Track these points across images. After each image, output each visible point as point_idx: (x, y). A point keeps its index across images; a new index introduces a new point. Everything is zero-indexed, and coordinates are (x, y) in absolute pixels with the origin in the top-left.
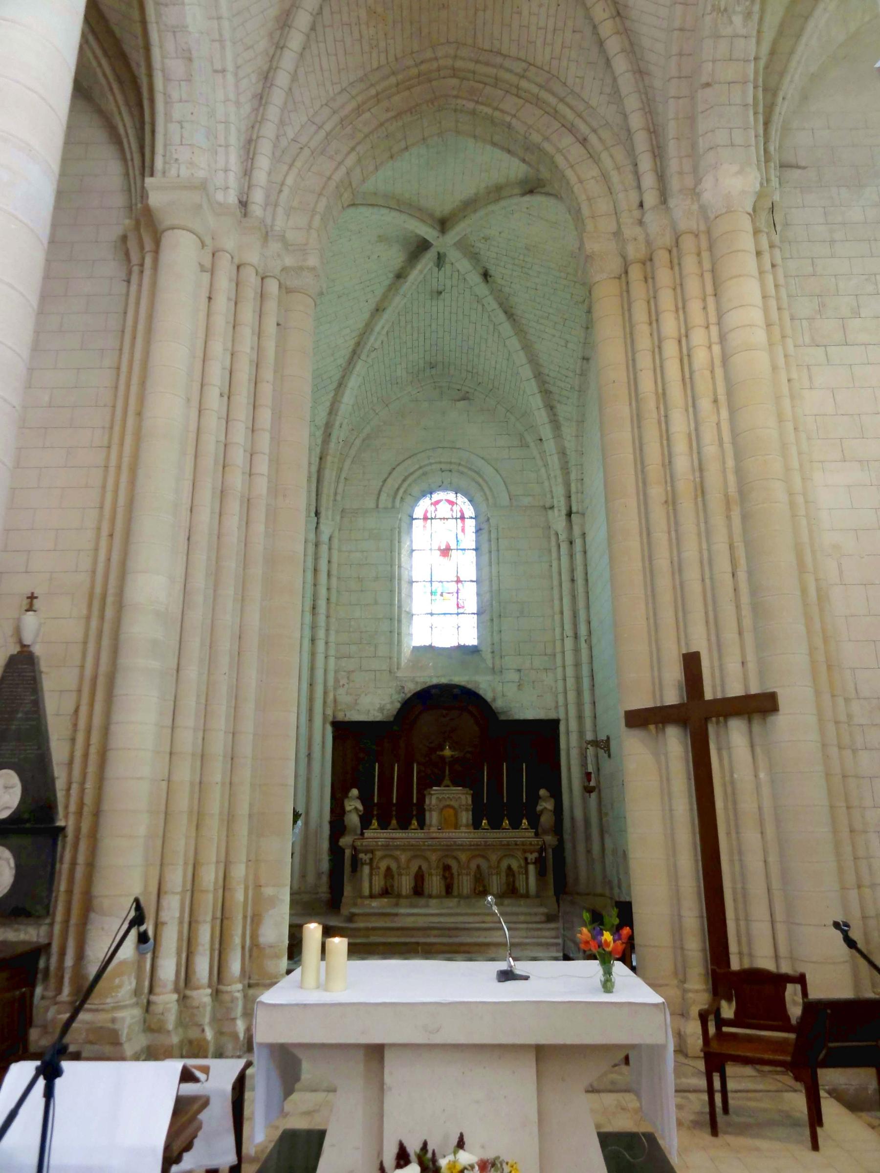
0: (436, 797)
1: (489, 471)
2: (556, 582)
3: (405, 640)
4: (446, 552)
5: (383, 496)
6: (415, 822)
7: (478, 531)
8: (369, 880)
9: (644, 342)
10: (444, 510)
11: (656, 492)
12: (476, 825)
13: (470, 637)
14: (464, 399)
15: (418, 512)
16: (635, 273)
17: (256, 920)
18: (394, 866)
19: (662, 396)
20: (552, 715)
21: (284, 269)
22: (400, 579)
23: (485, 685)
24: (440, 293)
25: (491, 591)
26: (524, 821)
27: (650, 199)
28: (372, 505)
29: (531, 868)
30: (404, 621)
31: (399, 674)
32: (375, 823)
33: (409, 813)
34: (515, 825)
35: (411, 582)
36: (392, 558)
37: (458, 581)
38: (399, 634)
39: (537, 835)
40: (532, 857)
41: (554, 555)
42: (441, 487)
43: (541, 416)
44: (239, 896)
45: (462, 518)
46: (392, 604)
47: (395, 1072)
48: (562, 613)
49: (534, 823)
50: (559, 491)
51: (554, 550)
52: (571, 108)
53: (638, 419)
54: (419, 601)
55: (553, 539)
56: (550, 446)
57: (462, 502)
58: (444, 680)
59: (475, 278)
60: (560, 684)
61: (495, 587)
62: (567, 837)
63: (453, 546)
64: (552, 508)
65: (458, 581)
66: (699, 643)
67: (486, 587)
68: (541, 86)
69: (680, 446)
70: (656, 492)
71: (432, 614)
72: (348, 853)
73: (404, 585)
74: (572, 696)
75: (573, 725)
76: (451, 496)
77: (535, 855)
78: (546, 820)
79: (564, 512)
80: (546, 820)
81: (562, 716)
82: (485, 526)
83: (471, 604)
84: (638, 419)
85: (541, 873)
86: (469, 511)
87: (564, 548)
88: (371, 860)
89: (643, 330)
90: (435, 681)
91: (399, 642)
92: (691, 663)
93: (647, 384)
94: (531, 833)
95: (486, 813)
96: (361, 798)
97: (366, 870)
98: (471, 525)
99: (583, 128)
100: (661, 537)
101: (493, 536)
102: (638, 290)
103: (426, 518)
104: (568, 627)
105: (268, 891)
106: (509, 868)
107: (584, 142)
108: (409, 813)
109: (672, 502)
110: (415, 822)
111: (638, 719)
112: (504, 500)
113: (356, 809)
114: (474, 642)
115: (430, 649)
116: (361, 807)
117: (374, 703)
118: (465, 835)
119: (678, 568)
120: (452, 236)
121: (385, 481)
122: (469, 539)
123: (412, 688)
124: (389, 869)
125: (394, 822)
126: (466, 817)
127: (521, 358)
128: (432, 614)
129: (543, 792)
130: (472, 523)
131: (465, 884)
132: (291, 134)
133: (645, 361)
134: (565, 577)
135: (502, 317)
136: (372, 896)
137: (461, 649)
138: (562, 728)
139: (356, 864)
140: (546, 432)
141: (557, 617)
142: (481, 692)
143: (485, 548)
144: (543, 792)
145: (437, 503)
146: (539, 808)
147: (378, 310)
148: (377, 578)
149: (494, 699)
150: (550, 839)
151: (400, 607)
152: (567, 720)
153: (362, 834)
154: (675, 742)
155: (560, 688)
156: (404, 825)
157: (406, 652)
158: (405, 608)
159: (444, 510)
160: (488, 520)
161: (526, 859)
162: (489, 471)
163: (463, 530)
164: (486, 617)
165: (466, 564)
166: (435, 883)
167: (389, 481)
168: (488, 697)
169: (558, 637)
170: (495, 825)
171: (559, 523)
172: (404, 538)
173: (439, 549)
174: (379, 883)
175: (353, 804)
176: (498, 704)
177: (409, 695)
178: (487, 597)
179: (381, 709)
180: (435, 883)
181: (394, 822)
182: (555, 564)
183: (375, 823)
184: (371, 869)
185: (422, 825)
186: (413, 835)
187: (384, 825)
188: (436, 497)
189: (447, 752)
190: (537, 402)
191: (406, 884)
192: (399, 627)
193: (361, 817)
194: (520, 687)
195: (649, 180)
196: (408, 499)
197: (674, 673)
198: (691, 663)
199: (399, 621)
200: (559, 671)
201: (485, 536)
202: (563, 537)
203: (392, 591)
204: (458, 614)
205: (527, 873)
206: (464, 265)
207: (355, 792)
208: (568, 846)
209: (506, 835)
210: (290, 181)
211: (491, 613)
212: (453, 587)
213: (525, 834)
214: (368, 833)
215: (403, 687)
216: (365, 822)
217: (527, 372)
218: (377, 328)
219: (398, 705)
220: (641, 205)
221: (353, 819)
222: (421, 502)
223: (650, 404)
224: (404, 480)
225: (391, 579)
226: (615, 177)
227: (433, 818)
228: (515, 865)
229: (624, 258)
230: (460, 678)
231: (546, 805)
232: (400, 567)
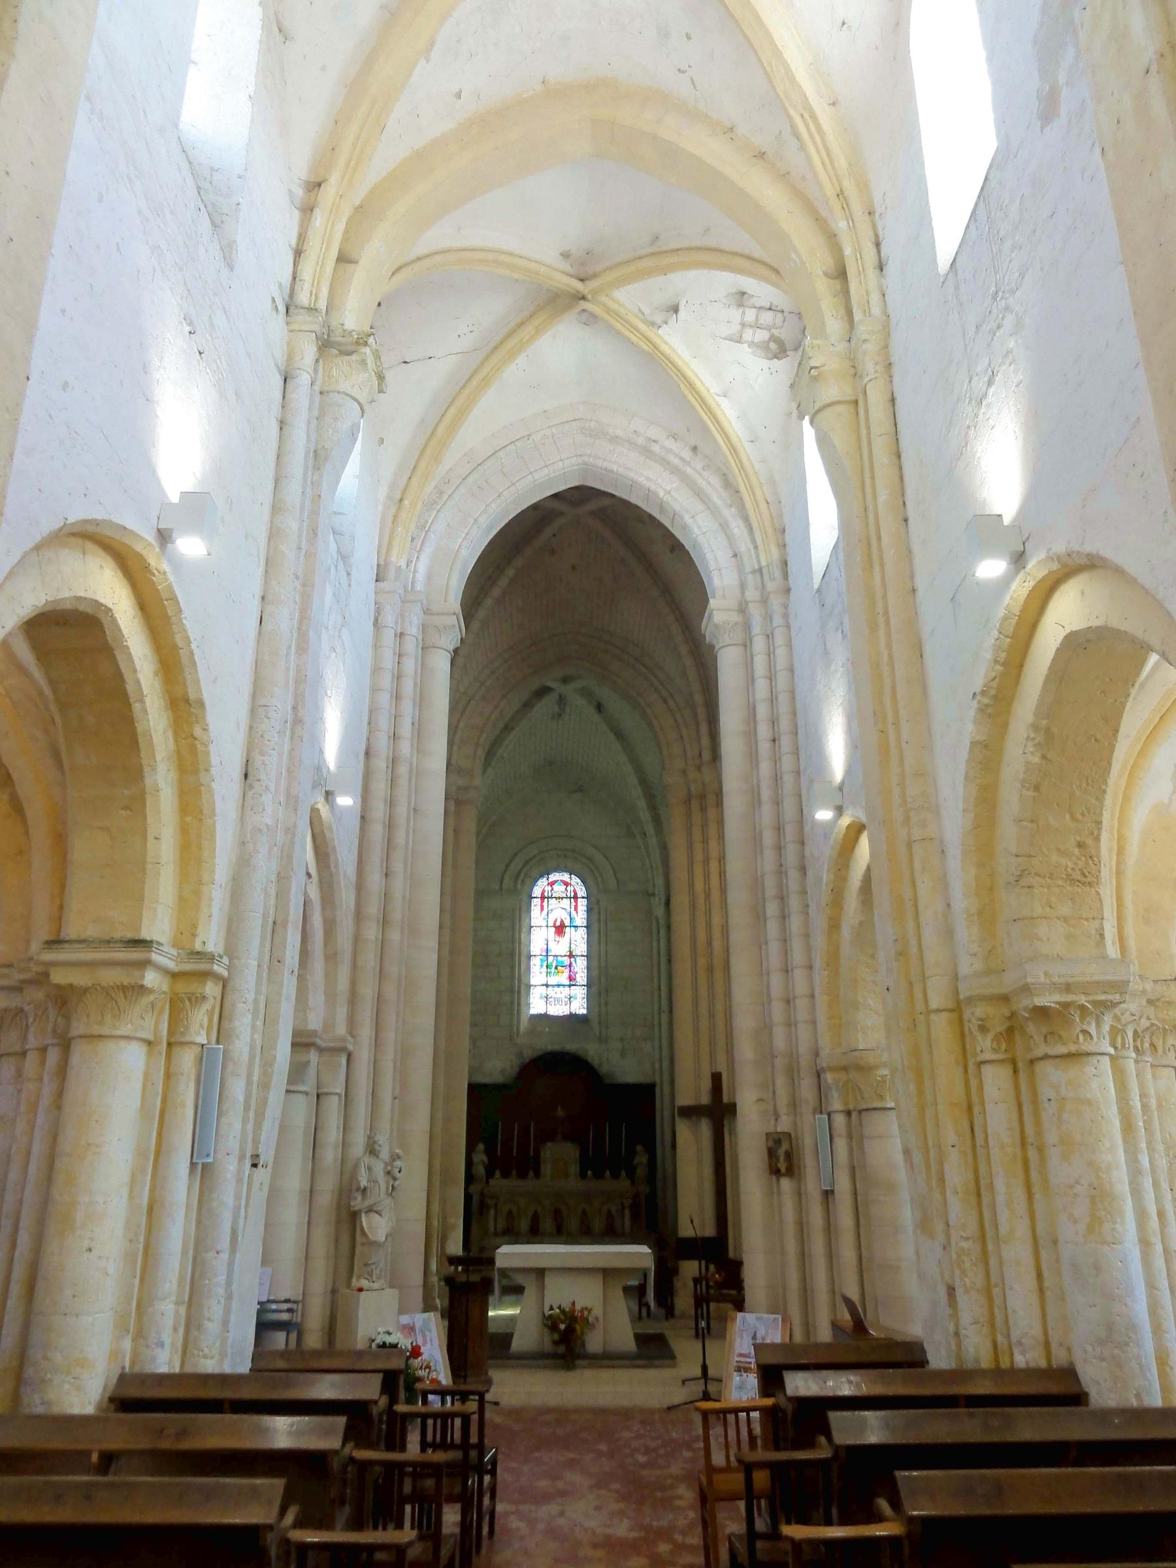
0: (550, 1151)
1: (598, 857)
2: (655, 961)
3: (523, 1009)
4: (560, 929)
5: (506, 881)
6: (531, 1174)
7: (589, 910)
8: (492, 1221)
9: (699, 856)
10: (559, 889)
11: (702, 962)
12: (583, 1175)
13: (579, 1007)
14: (580, 790)
15: (537, 891)
16: (695, 804)
17: (444, 1239)
18: (514, 1210)
19: (708, 895)
20: (648, 1080)
21: (459, 788)
22: (520, 955)
23: (592, 1051)
24: (560, 715)
25: (599, 967)
26: (623, 1173)
27: (707, 756)
28: (497, 888)
29: (627, 1212)
30: (523, 991)
31: (519, 1041)
32: (498, 1174)
33: (527, 1165)
34: (615, 1176)
35: (529, 957)
36: (513, 936)
37: (571, 956)
38: (519, 1005)
39: (633, 1183)
40: (628, 1202)
41: (655, 937)
42: (558, 869)
43: (645, 816)
44: (435, 1223)
45: (576, 898)
46: (513, 978)
47: (549, 1280)
48: (659, 989)
49: (631, 1176)
50: (660, 881)
51: (655, 931)
52: (656, 677)
53: (693, 906)
54: (537, 975)
55: (654, 923)
56: (653, 841)
57: (575, 880)
58: (557, 1047)
59: (590, 710)
60: (657, 1052)
61: (603, 965)
62: (659, 1185)
63: (567, 923)
64: (653, 894)
65: (571, 956)
66: (722, 1068)
67: (595, 963)
68: (636, 659)
69: (717, 935)
70: (702, 962)
71: (547, 986)
72: (476, 1199)
73: (523, 959)
74: (666, 1064)
75: (667, 1090)
76: (566, 877)
77: (631, 1201)
78: (641, 1172)
79: (663, 901)
80: (641, 1172)
81: (658, 1080)
82: (596, 907)
83: (582, 977)
84: (693, 906)
85: (635, 1217)
86: (582, 891)
87: (663, 932)
88: (496, 1205)
89: (698, 846)
90: (550, 1048)
91: (519, 1011)
92: (716, 1078)
93: (699, 886)
94: (628, 1183)
95: (592, 1165)
96: (487, 1152)
97: (492, 1212)
98: (582, 904)
99: (664, 692)
100: (703, 992)
101: (603, 917)
102: (697, 818)
103: (543, 898)
104: (664, 1002)
105: (452, 1220)
106: (609, 1212)
107: (665, 702)
108: (527, 1165)
109: (710, 970)
110: (531, 1174)
111: (689, 1112)
112: (612, 884)
113: (483, 1162)
114: (584, 1011)
115: (545, 1017)
116: (484, 1158)
117: (499, 1067)
118: (574, 1183)
119: (712, 1015)
120: (572, 686)
121: (508, 865)
122: (581, 918)
123: (528, 1054)
124: (510, 1213)
125: (514, 1173)
126: (574, 1169)
127: (628, 768)
128: (547, 986)
129: (639, 1148)
130: (585, 902)
131: (573, 1224)
132: (462, 689)
133: (699, 870)
134: (663, 959)
135: (612, 737)
136: (496, 1234)
137: (572, 1017)
138: (658, 1090)
139: (483, 1207)
140: (650, 829)
141: (656, 994)
142: (589, 1059)
143: (595, 926)
144: (639, 1148)
145: (552, 884)
146: (635, 1162)
147: (508, 728)
148: (500, 955)
149: (600, 1065)
150: (644, 1189)
151: (520, 981)
152: (662, 1082)
153: (488, 1182)
154: (705, 1128)
155: (657, 1057)
156: (522, 1175)
157: (524, 1023)
158: (524, 980)
159: (559, 889)
160: (598, 902)
161: (622, 1204)
162: (598, 857)
163: (576, 909)
164: (595, 989)
165: (578, 940)
166: (547, 1224)
167: (513, 865)
168: (595, 1062)
169: (656, 1011)
170: (599, 1176)
171: (659, 911)
172: (523, 915)
173: (554, 926)
174: (501, 1224)
175: (480, 1157)
176: (604, 1069)
177: (527, 1061)
178: (595, 973)
179: (503, 1072)
180: (547, 1224)
181: (514, 1173)
182: (655, 944)
183: (498, 1174)
184: (496, 1213)
185: (537, 1175)
186: (529, 1184)
187: (505, 1175)
188: (554, 877)
189: (560, 1112)
190: (641, 804)
191: (524, 1224)
192: (519, 998)
193: (486, 1168)
194: (623, 1054)
195: (705, 741)
196: (528, 881)
197: (706, 1084)
198: (716, 1078)
199: (519, 992)
200: (657, 1043)
201: (595, 917)
202: (662, 922)
203: (513, 967)
204: (570, 986)
205: (623, 1218)
206: (581, 702)
207: (481, 1147)
208: (660, 1194)
209: (608, 1184)
210: (462, 725)
211: (598, 986)
212: (566, 961)
213: (624, 1184)
214: (492, 1182)
215: (521, 1053)
216: (490, 1174)
217: (633, 780)
218: (506, 742)
219: (517, 1069)
220: (700, 755)
221: (480, 1170)
222: (539, 883)
223: (701, 900)
224: (524, 865)
225: (512, 955)
226: (684, 731)
227: (547, 1169)
228: (614, 1209)
229: (689, 790)
230: (571, 1047)
231: (642, 1159)
232: (520, 943)
